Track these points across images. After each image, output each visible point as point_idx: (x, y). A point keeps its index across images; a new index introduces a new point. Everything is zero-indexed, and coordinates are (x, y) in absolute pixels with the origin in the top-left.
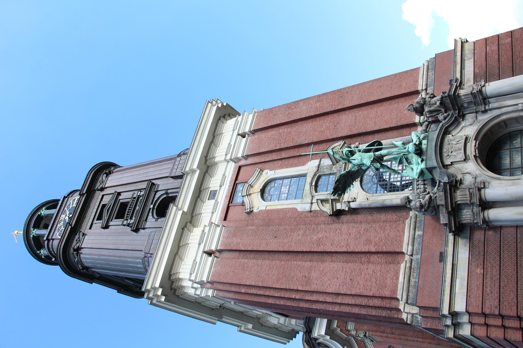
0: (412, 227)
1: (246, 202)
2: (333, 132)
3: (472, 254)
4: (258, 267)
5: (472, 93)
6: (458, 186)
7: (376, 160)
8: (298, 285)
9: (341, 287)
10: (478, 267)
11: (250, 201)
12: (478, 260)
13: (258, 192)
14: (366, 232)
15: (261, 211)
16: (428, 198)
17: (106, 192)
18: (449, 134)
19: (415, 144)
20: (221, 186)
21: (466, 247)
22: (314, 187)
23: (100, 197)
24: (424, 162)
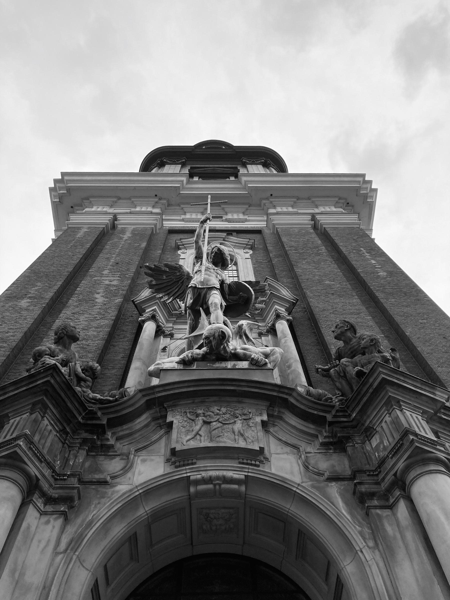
7: (199, 295)
18: (269, 415)
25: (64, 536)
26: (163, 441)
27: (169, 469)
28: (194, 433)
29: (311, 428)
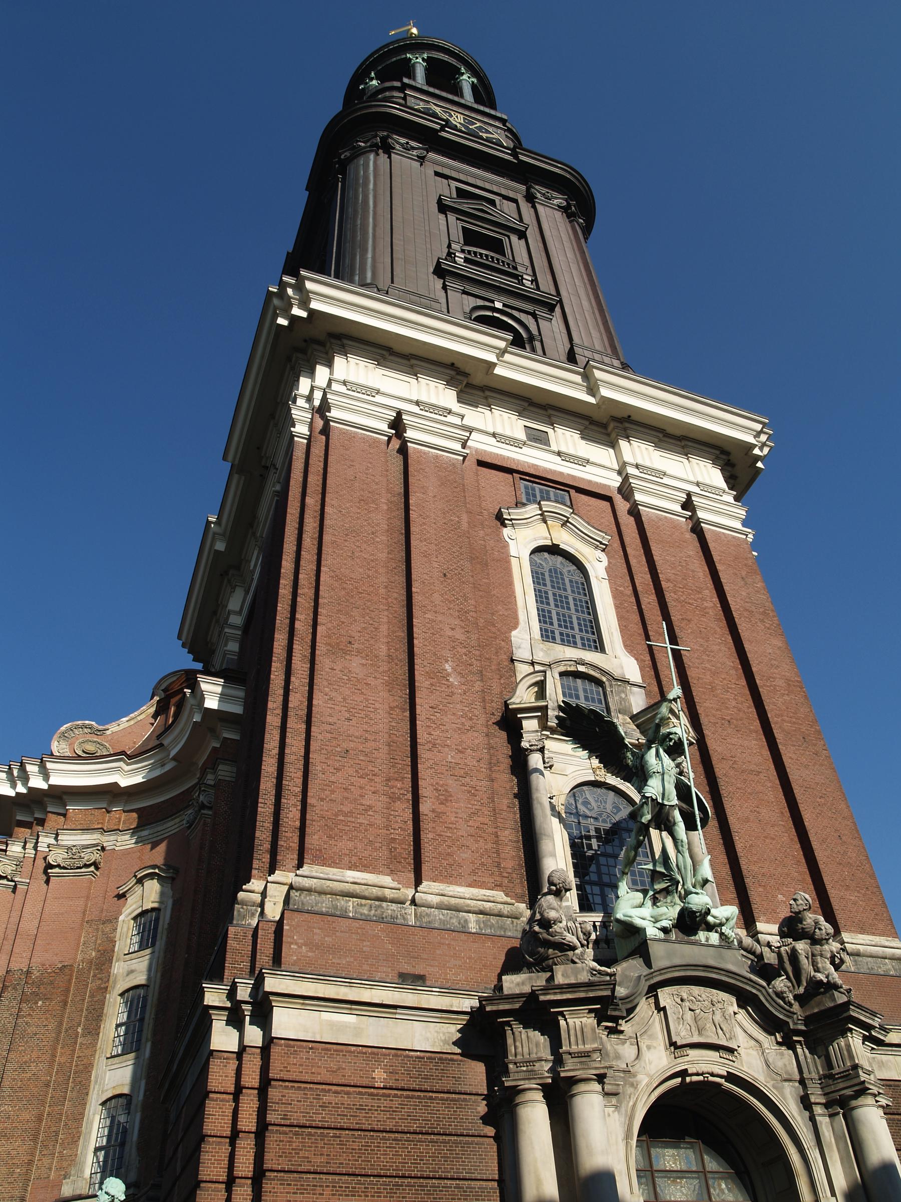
0: (488, 906)
1: (527, 509)
2: (714, 716)
3: (423, 1058)
4: (369, 534)
5: (855, 1067)
8: (330, 625)
9: (328, 727)
10: (390, 1073)
12: (407, 1074)
13: (551, 540)
14: (469, 792)
15: (506, 546)
16: (570, 940)
17: (525, 207)
19: (708, 912)
20: (559, 454)
21: (442, 1044)
22: (573, 669)
23: (511, 194)
24: (661, 935)
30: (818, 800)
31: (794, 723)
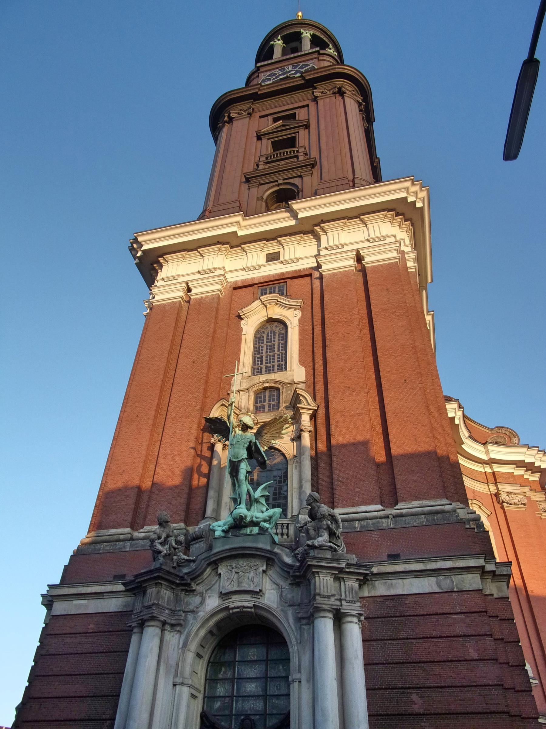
6: (181, 588)
7: (234, 465)
11: (255, 311)
15: (241, 329)
18: (267, 565)
24: (223, 535)
25: (181, 641)
26: (218, 583)
27: (221, 602)
28: (231, 580)
29: (285, 575)
30: (405, 419)
31: (400, 373)
